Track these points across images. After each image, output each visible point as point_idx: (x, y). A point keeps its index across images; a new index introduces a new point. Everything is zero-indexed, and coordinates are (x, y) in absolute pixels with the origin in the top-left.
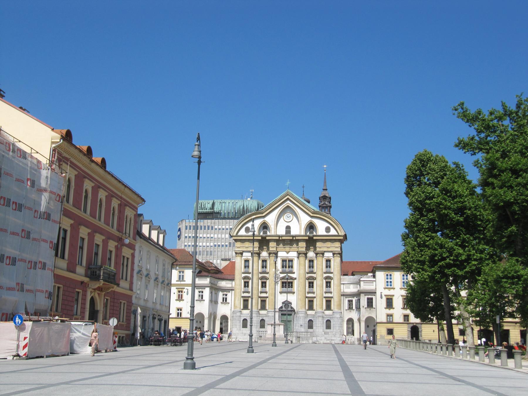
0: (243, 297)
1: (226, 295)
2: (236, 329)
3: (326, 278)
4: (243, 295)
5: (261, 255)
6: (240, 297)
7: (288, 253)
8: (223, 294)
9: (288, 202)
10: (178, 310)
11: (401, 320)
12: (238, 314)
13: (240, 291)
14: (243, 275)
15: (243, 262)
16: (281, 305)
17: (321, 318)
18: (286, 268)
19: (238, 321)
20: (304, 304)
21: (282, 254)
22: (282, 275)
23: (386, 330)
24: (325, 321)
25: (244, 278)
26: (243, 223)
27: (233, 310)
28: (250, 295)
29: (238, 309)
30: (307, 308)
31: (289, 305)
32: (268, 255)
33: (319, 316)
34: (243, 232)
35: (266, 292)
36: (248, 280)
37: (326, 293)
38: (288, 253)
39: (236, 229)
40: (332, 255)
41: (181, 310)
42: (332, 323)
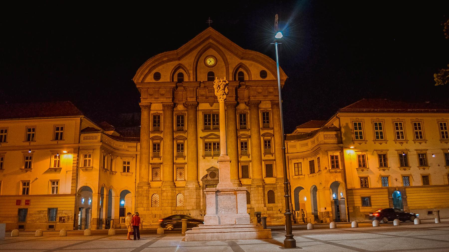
0: (151, 164)
1: (129, 163)
2: (142, 209)
3: (264, 135)
4: (151, 161)
5: (175, 109)
6: (147, 165)
7: (211, 106)
8: (124, 163)
9: (211, 41)
10: (53, 183)
11: (380, 185)
12: (146, 188)
13: (147, 156)
14: (152, 135)
15: (151, 118)
16: (206, 173)
17: (261, 189)
18: (209, 124)
19: (145, 198)
20: (236, 171)
21: (204, 106)
22: (206, 134)
23: (360, 199)
24: (266, 193)
25: (153, 139)
26: (150, 67)
27: (138, 182)
28: (161, 161)
29: (145, 180)
30: (240, 176)
31: (216, 172)
32: (186, 109)
33: (258, 186)
34: (150, 79)
35: (184, 157)
36: (159, 141)
37: (265, 154)
38: (211, 106)
39: (142, 74)
40: (270, 106)
41: (57, 184)
42: (276, 195)
